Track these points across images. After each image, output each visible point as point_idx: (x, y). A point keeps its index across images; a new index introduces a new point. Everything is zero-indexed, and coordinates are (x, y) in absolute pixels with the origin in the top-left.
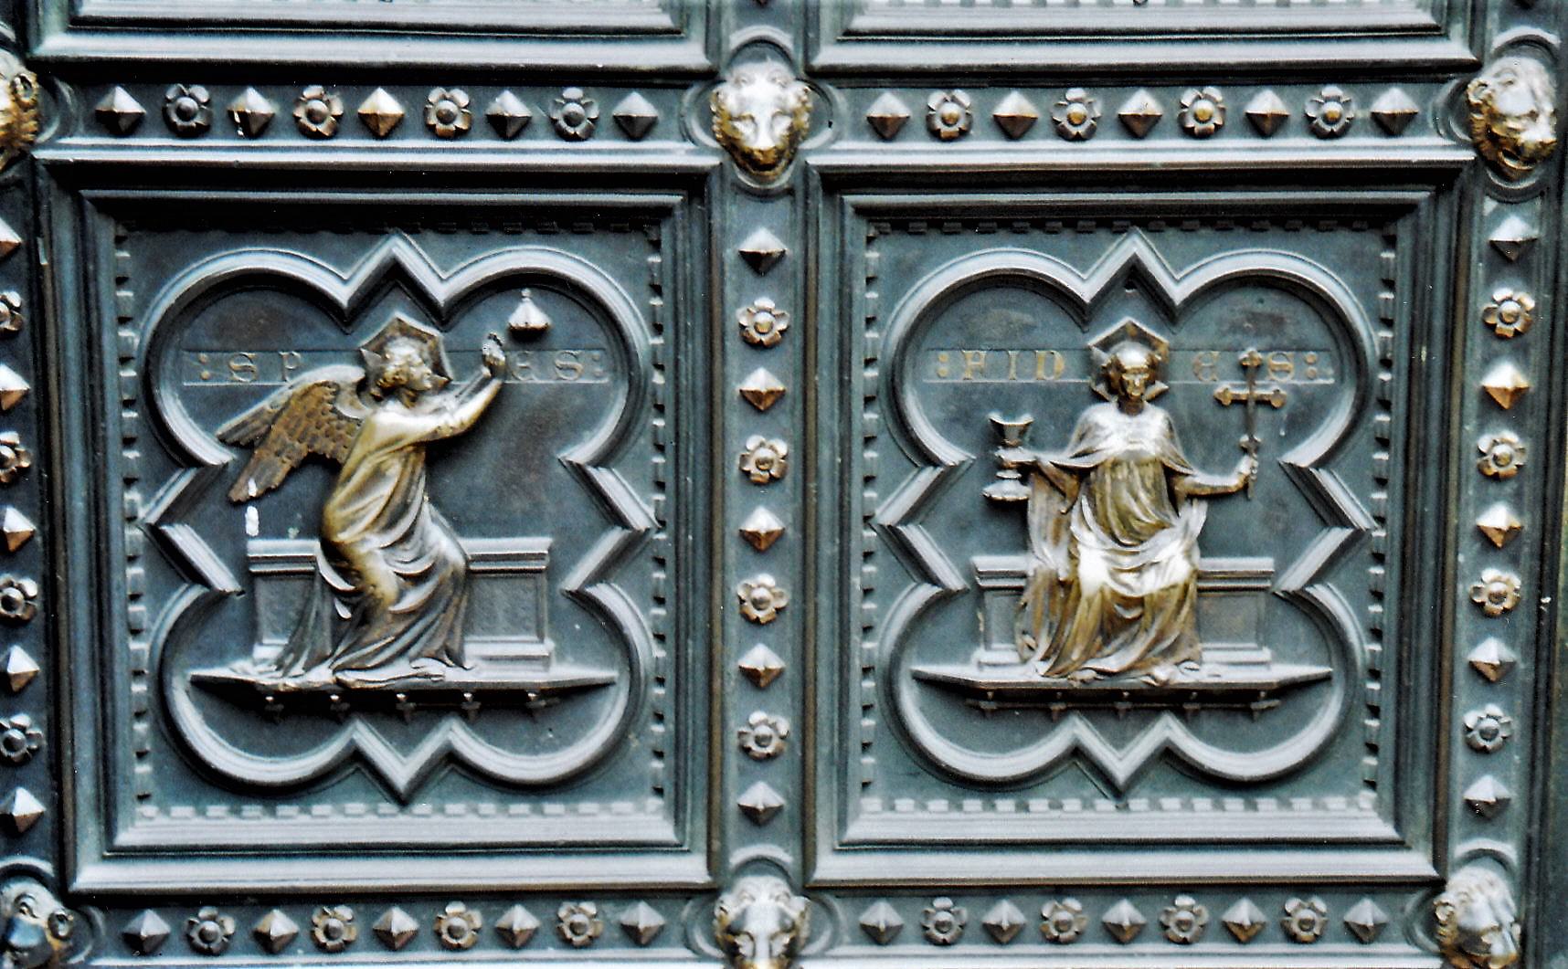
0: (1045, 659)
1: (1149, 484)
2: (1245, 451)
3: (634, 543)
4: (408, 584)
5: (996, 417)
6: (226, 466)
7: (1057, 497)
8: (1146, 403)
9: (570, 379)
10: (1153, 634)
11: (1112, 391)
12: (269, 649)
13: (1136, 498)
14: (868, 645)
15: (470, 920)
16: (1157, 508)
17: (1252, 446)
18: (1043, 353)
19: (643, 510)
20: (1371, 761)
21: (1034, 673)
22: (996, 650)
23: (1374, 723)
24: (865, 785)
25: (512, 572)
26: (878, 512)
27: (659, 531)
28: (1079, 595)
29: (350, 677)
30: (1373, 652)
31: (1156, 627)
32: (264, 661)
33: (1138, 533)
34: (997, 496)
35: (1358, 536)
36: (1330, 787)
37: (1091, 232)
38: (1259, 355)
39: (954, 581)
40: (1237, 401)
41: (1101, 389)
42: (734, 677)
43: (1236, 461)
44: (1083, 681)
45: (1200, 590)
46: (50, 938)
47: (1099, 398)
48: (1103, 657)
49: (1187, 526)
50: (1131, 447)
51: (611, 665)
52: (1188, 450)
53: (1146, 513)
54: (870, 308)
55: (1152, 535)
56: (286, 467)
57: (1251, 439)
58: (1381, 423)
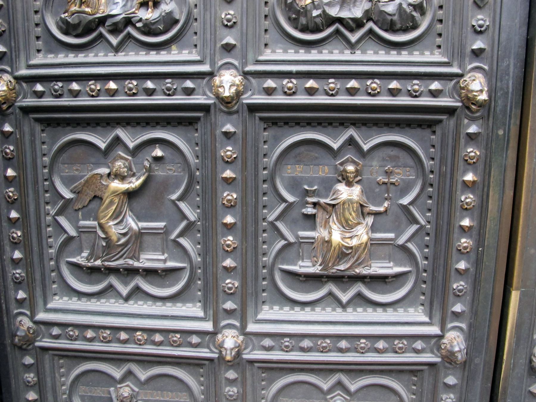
0: (320, 265)
1: (355, 209)
2: (386, 199)
3: (190, 225)
4: (122, 236)
5: (306, 187)
6: (72, 199)
7: (325, 213)
8: (355, 184)
9: (170, 173)
10: (355, 258)
11: (344, 179)
12: (85, 254)
13: (351, 214)
14: (264, 259)
15: (143, 336)
16: (357, 217)
17: (389, 198)
18: (321, 166)
19: (193, 215)
20: (423, 297)
21: (316, 269)
22: (305, 262)
23: (424, 286)
24: (263, 302)
25: (153, 233)
26: (268, 217)
27: (199, 221)
28: (331, 246)
29: (106, 263)
30: (425, 264)
31: (356, 255)
32: (83, 257)
33: (352, 226)
34: (306, 213)
35: (422, 227)
36: (410, 306)
37: (337, 127)
38: (391, 168)
39: (292, 239)
40: (384, 183)
41: (340, 178)
42: (221, 268)
43: (384, 202)
44: (332, 273)
45: (371, 244)
46: (28, 334)
47: (340, 182)
48: (339, 265)
49: (367, 224)
50: (349, 197)
51: (185, 263)
52: (368, 198)
53: (353, 218)
54: (265, 151)
55: (355, 227)
56: (88, 200)
57: (388, 195)
58: (429, 191)
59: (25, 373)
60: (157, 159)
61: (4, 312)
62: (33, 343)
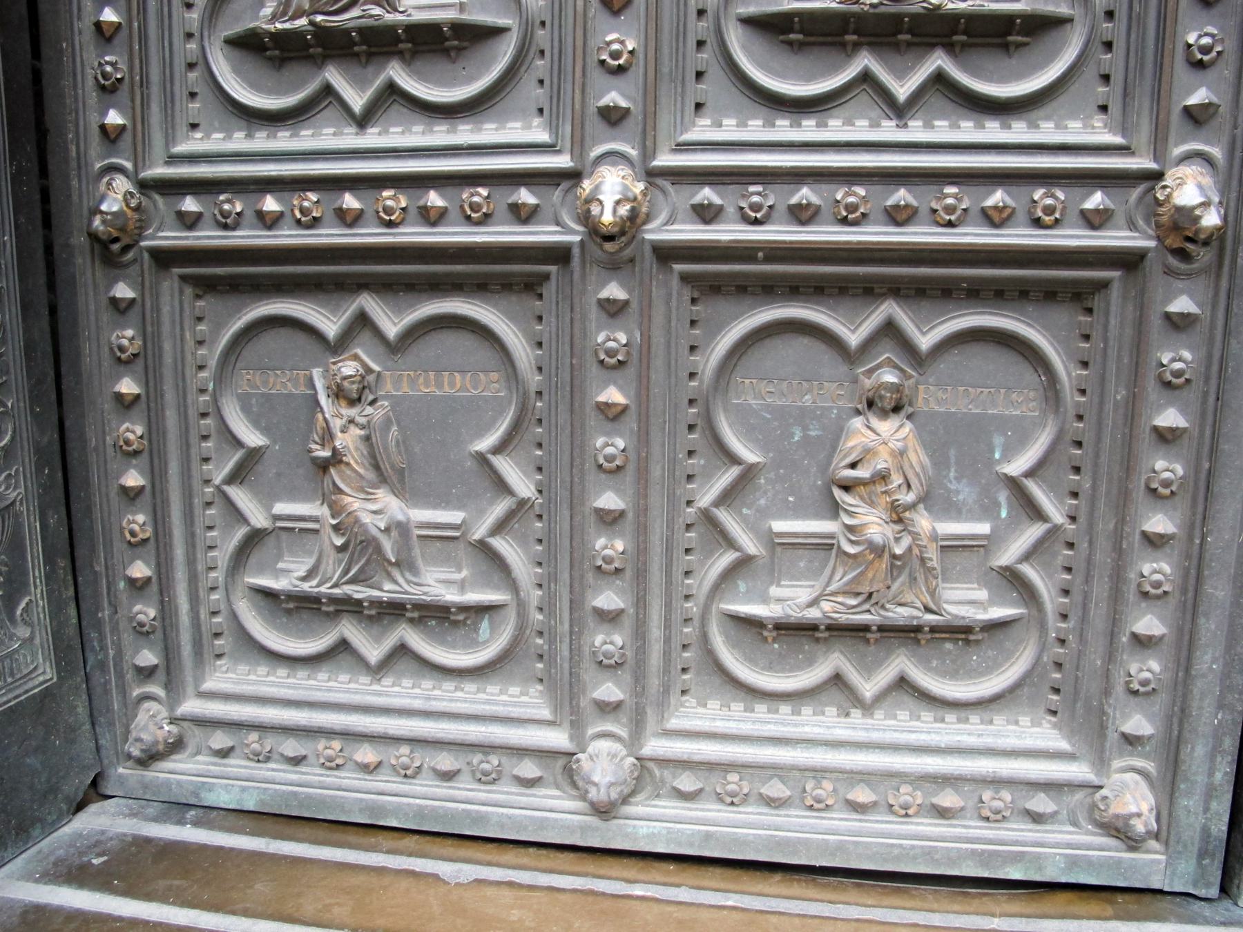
59: (113, 330)
61: (74, 164)
62: (137, 242)
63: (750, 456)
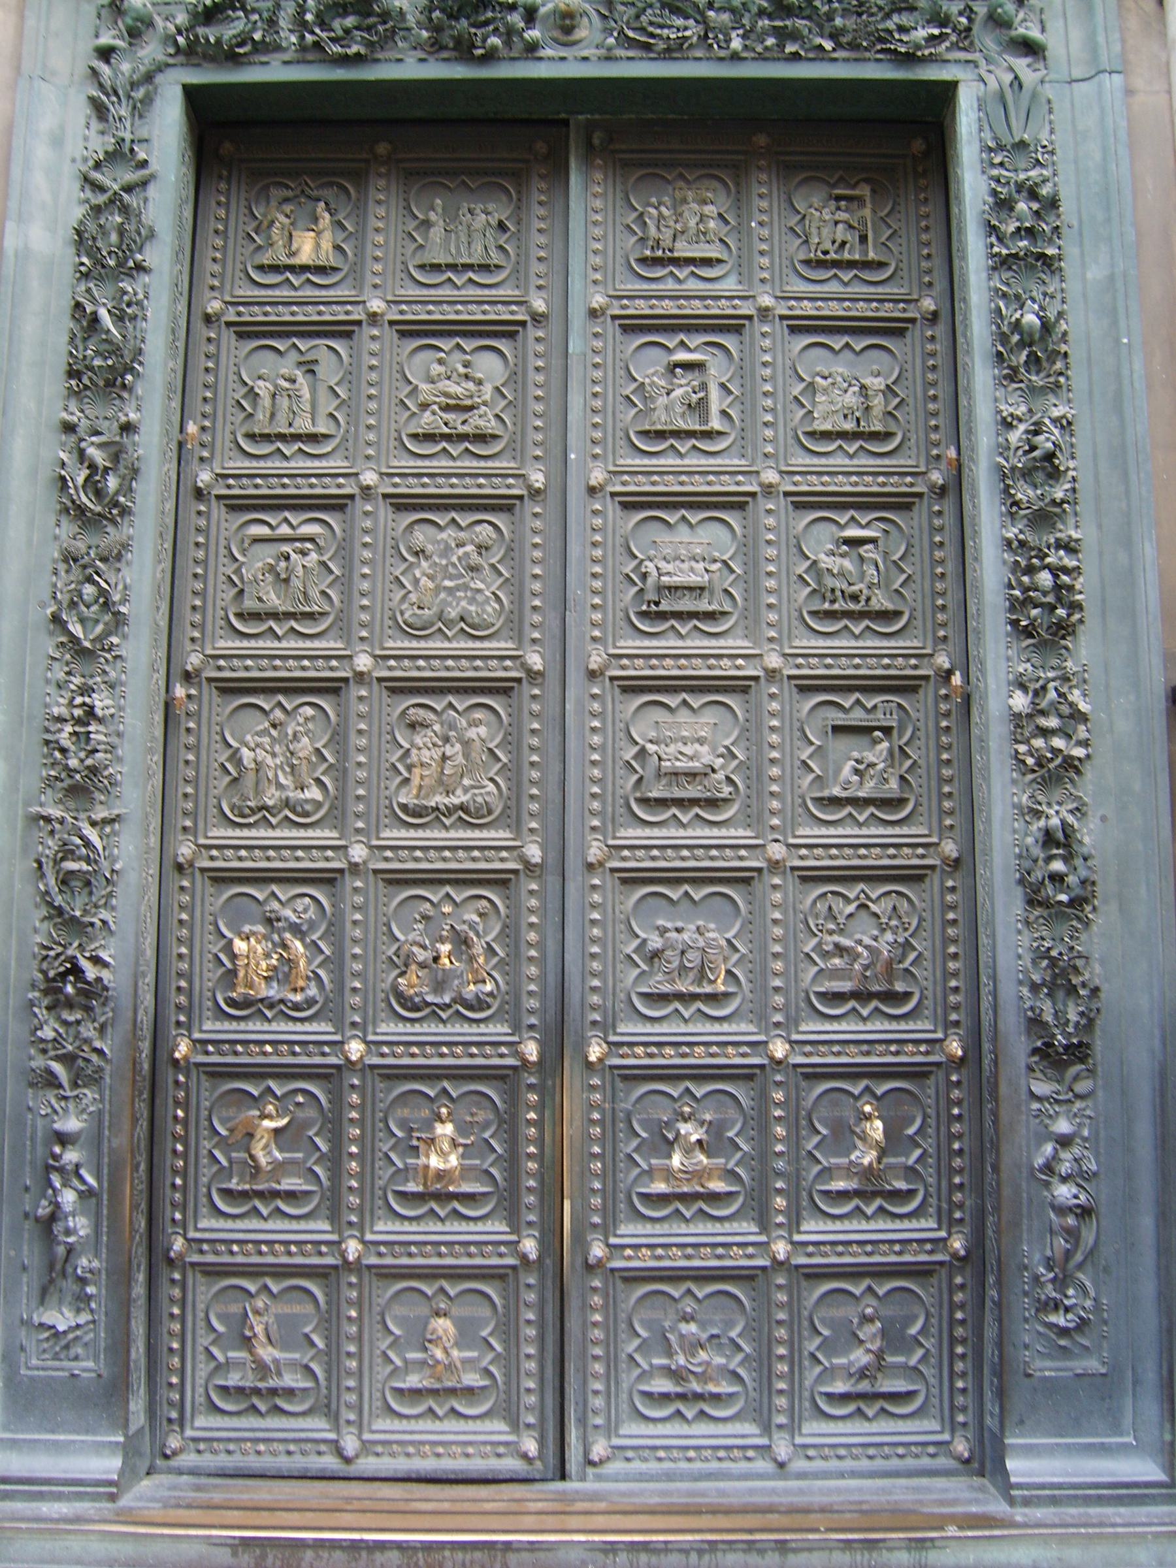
3: (323, 1155)
12: (234, 1181)
21: (420, 1189)
25: (293, 1162)
60: (298, 1104)
63: (397, 1332)
